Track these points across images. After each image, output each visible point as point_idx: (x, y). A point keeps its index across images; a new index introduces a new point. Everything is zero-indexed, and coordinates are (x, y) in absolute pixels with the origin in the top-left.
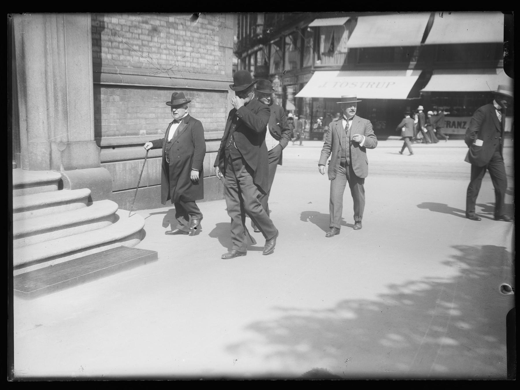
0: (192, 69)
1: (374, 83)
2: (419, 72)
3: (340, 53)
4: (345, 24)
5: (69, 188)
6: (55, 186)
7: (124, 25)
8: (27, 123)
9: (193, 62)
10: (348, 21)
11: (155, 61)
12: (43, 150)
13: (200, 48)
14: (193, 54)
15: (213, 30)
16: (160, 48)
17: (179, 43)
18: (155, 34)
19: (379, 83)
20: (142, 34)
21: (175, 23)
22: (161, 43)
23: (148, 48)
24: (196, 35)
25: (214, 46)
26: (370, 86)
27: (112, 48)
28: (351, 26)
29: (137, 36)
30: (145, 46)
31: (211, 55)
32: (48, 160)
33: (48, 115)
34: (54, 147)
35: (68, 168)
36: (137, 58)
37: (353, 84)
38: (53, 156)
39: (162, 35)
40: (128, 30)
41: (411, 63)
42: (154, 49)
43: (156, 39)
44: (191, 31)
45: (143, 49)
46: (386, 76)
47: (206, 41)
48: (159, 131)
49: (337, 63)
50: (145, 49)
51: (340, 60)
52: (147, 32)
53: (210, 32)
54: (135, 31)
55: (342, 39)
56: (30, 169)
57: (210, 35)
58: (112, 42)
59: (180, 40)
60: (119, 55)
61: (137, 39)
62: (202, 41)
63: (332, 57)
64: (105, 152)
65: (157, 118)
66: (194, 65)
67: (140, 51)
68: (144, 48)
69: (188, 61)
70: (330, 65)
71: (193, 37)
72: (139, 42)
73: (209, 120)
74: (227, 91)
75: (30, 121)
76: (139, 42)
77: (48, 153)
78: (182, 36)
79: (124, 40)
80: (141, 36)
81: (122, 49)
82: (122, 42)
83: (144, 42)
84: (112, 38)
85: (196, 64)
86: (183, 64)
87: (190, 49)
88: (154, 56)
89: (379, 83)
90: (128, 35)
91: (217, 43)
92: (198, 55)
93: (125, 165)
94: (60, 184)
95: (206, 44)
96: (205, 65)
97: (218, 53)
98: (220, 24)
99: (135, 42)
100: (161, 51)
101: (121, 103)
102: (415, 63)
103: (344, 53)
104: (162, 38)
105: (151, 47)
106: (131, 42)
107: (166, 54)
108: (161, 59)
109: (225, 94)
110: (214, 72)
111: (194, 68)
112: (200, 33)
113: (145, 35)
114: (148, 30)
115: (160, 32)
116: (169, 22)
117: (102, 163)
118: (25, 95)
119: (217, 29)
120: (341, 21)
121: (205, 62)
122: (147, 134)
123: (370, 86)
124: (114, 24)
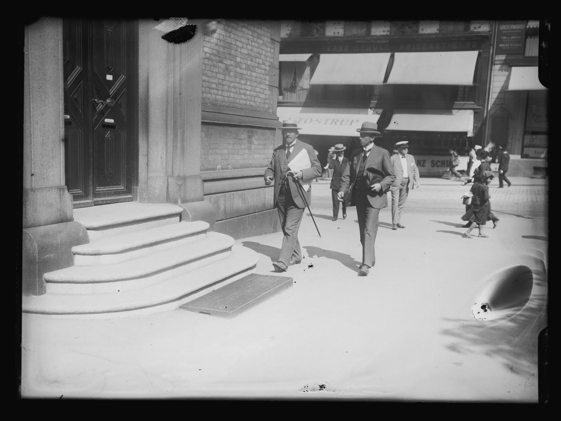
0: (250, 107)
1: (338, 120)
2: (380, 111)
3: (302, 89)
4: (307, 60)
5: (188, 220)
6: (178, 218)
8: (148, 158)
10: (311, 58)
11: (226, 99)
12: (162, 183)
14: (252, 93)
15: (265, 70)
16: (229, 86)
17: (243, 82)
19: (343, 121)
21: (241, 63)
22: (231, 82)
24: (254, 74)
26: (334, 123)
28: (313, 63)
30: (219, 84)
32: (165, 194)
33: (167, 150)
34: (170, 180)
35: (184, 201)
37: (317, 121)
38: (170, 189)
39: (232, 74)
41: (372, 101)
46: (348, 113)
47: (260, 80)
48: (230, 166)
49: (299, 99)
50: (220, 87)
51: (303, 97)
53: (263, 71)
54: (214, 70)
55: (304, 75)
56: (148, 202)
62: (258, 80)
63: (294, 93)
64: (207, 184)
65: (229, 154)
66: (252, 103)
67: (217, 89)
70: (292, 101)
72: (216, 81)
73: (263, 156)
74: (275, 129)
75: (150, 156)
76: (216, 81)
77: (166, 186)
79: (207, 79)
80: (218, 75)
81: (205, 87)
86: (245, 102)
88: (225, 94)
89: (343, 121)
90: (210, 74)
91: (267, 83)
92: (255, 94)
93: (210, 198)
94: (180, 216)
95: (260, 83)
97: (268, 92)
101: (206, 139)
102: (376, 102)
103: (306, 89)
105: (224, 85)
109: (274, 131)
111: (252, 106)
117: (205, 195)
118: (147, 132)
119: (268, 68)
120: (304, 57)
122: (222, 169)
123: (334, 123)
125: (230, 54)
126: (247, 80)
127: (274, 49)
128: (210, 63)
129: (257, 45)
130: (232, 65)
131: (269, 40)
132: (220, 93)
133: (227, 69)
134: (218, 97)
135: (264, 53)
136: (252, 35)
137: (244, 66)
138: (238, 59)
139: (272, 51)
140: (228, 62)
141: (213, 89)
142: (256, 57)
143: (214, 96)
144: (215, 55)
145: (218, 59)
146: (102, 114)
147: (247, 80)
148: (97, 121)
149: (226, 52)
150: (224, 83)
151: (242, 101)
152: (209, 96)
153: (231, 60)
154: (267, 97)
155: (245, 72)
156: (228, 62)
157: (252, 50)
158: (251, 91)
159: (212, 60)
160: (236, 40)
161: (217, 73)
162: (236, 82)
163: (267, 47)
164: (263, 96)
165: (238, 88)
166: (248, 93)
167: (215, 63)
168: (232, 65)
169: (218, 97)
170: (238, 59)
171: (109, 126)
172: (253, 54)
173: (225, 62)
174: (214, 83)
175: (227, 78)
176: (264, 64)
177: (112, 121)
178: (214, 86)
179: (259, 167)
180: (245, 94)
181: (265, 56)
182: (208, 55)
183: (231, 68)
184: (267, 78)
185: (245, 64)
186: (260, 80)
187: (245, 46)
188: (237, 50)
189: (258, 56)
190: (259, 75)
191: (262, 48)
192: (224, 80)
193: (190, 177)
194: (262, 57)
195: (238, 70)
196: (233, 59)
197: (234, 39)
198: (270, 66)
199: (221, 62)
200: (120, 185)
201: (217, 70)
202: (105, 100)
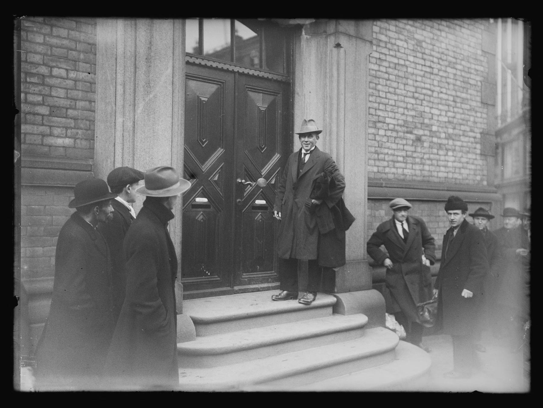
0: (454, 180)
6: (330, 310)
7: (390, 136)
9: (455, 172)
11: (418, 173)
14: (456, 164)
15: (475, 138)
16: (422, 158)
17: (441, 152)
18: (419, 144)
20: (406, 144)
21: (438, 131)
22: (424, 154)
23: (411, 159)
24: (459, 143)
25: (476, 154)
27: (378, 160)
29: (401, 147)
31: (473, 164)
36: (402, 170)
39: (426, 144)
43: (419, 149)
44: (453, 140)
45: (407, 160)
47: (468, 149)
50: (409, 160)
52: (411, 142)
53: (472, 140)
54: (401, 142)
57: (472, 143)
58: (378, 154)
59: (442, 149)
60: (384, 167)
62: (465, 149)
66: (456, 176)
67: (404, 162)
68: (408, 158)
71: (455, 146)
76: (404, 153)
78: (445, 145)
79: (390, 152)
81: (388, 161)
82: (387, 154)
83: (408, 153)
85: (458, 175)
87: (452, 159)
88: (417, 167)
90: (394, 146)
91: (478, 152)
92: (460, 165)
95: (468, 152)
96: (467, 175)
97: (480, 162)
98: (481, 130)
99: (400, 153)
100: (424, 161)
104: (426, 147)
105: (415, 158)
107: (429, 165)
108: (424, 170)
110: (476, 182)
111: (456, 179)
112: (462, 142)
113: (409, 145)
115: (423, 142)
116: (432, 131)
119: (478, 136)
121: (467, 171)
125: (422, 124)
126: (447, 150)
127: (487, 114)
128: (394, 134)
129: (461, 111)
130: (424, 135)
131: (479, 104)
133: (419, 139)
134: (406, 171)
135: (472, 119)
136: (454, 101)
137: (443, 135)
138: (434, 128)
139: (484, 116)
141: (398, 162)
142: (461, 124)
143: (400, 171)
144: (401, 126)
145: (405, 129)
146: (252, 196)
147: (447, 150)
149: (417, 121)
150: (415, 155)
152: (394, 170)
153: (424, 130)
154: (479, 167)
155: (445, 142)
156: (421, 132)
157: (454, 117)
158: (454, 161)
159: (397, 132)
160: (431, 108)
162: (432, 154)
163: (476, 112)
164: (473, 167)
165: (435, 159)
166: (450, 164)
167: (401, 134)
168: (424, 135)
169: (406, 171)
171: (261, 207)
172: (455, 121)
173: (415, 132)
175: (419, 149)
176: (472, 131)
177: (263, 202)
178: (400, 159)
180: (446, 166)
181: (475, 122)
182: (391, 127)
184: (478, 146)
185: (445, 133)
186: (468, 149)
187: (443, 113)
188: (432, 119)
189: (464, 122)
190: (465, 144)
191: (469, 113)
192: (415, 152)
194: (469, 123)
195: (435, 140)
196: (426, 128)
197: (427, 106)
198: (481, 133)
199: (411, 133)
201: (404, 142)
202: (255, 180)
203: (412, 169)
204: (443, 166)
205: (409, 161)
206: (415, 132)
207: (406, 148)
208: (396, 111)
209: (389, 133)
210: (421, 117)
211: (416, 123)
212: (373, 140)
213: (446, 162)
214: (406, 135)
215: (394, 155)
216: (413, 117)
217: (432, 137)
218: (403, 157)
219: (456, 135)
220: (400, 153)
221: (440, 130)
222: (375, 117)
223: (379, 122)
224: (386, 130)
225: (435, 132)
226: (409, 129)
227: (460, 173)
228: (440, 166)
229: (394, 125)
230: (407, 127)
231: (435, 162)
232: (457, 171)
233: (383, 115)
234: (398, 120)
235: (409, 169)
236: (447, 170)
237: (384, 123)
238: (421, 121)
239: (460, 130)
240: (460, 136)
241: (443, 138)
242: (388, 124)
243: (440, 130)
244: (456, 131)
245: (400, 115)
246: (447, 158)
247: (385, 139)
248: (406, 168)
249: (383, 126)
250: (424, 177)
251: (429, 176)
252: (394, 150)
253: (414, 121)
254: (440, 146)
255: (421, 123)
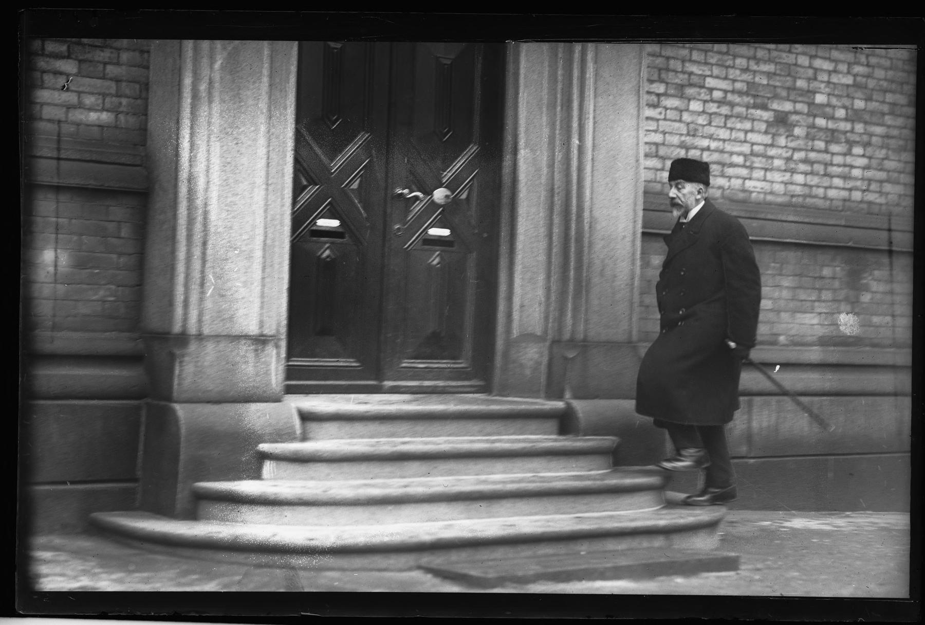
7: (715, 113)
9: (867, 190)
13: (886, 158)
14: (869, 174)
17: (835, 148)
18: (782, 130)
20: (752, 131)
22: (794, 150)
23: (764, 160)
24: (879, 130)
29: (741, 135)
30: (757, 155)
36: (740, 181)
39: (797, 131)
40: (722, 124)
42: (777, 163)
43: (782, 141)
44: (866, 123)
45: (753, 162)
50: (758, 162)
52: (763, 127)
54: (739, 126)
59: (838, 142)
61: (741, 141)
65: (778, 312)
66: (871, 197)
68: (755, 159)
69: (857, 189)
76: (746, 149)
79: (714, 145)
83: (756, 148)
84: (688, 140)
85: (877, 195)
87: (863, 162)
88: (777, 176)
90: (724, 134)
92: (882, 175)
99: (737, 148)
104: (798, 138)
105: (772, 158)
106: (728, 147)
108: (792, 183)
111: (870, 203)
113: (759, 132)
114: (767, 122)
116: (813, 103)
124: (693, 112)
128: (725, 110)
130: (796, 113)
132: (758, 174)
134: (749, 184)
137: (841, 113)
138: (820, 99)
140: (787, 106)
141: (732, 165)
143: (737, 183)
144: (740, 93)
147: (851, 144)
148: (411, 231)
149: (778, 84)
150: (772, 152)
151: (832, 193)
153: (795, 102)
156: (787, 106)
157: (868, 76)
159: (732, 105)
161: (746, 132)
162: (812, 150)
165: (819, 162)
167: (738, 110)
168: (796, 113)
169: (749, 184)
170: (820, 99)
171: (439, 241)
172: (871, 83)
174: (739, 154)
175: (782, 141)
178: (739, 160)
179: (890, 346)
180: (845, 177)
182: (717, 95)
183: (794, 118)
187: (843, 67)
188: (815, 79)
192: (772, 145)
193: (599, 344)
196: (800, 99)
199: (764, 107)
200: (458, 359)
201: (748, 125)
202: (428, 192)
203: (765, 180)
204: (838, 176)
205: (756, 165)
206: (775, 106)
207: (751, 137)
208: (730, 63)
209: (713, 108)
210: (789, 75)
211: (775, 87)
212: (675, 121)
213: (847, 169)
214: (752, 111)
215: (722, 151)
216: (769, 75)
217: (815, 116)
218: (745, 156)
219: (872, 113)
220: (737, 148)
221: (834, 101)
222: (681, 76)
223: (691, 85)
224: (705, 102)
225: (822, 106)
226: (759, 101)
227: (880, 193)
228: (832, 177)
229: (726, 92)
230: (755, 96)
231: (819, 168)
232: (874, 186)
233: (700, 72)
234: (734, 81)
235: (758, 180)
236: (850, 184)
237: (702, 87)
238: (788, 84)
239: (883, 102)
240: (883, 114)
241: (841, 120)
242: (711, 90)
243: (834, 101)
244: (873, 105)
245: (738, 72)
246: (849, 160)
247: (701, 120)
248: (750, 179)
249: (699, 94)
250: (792, 196)
251: (805, 196)
252: (724, 141)
253: (771, 83)
254: (832, 136)
255: (788, 89)
